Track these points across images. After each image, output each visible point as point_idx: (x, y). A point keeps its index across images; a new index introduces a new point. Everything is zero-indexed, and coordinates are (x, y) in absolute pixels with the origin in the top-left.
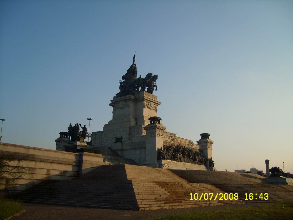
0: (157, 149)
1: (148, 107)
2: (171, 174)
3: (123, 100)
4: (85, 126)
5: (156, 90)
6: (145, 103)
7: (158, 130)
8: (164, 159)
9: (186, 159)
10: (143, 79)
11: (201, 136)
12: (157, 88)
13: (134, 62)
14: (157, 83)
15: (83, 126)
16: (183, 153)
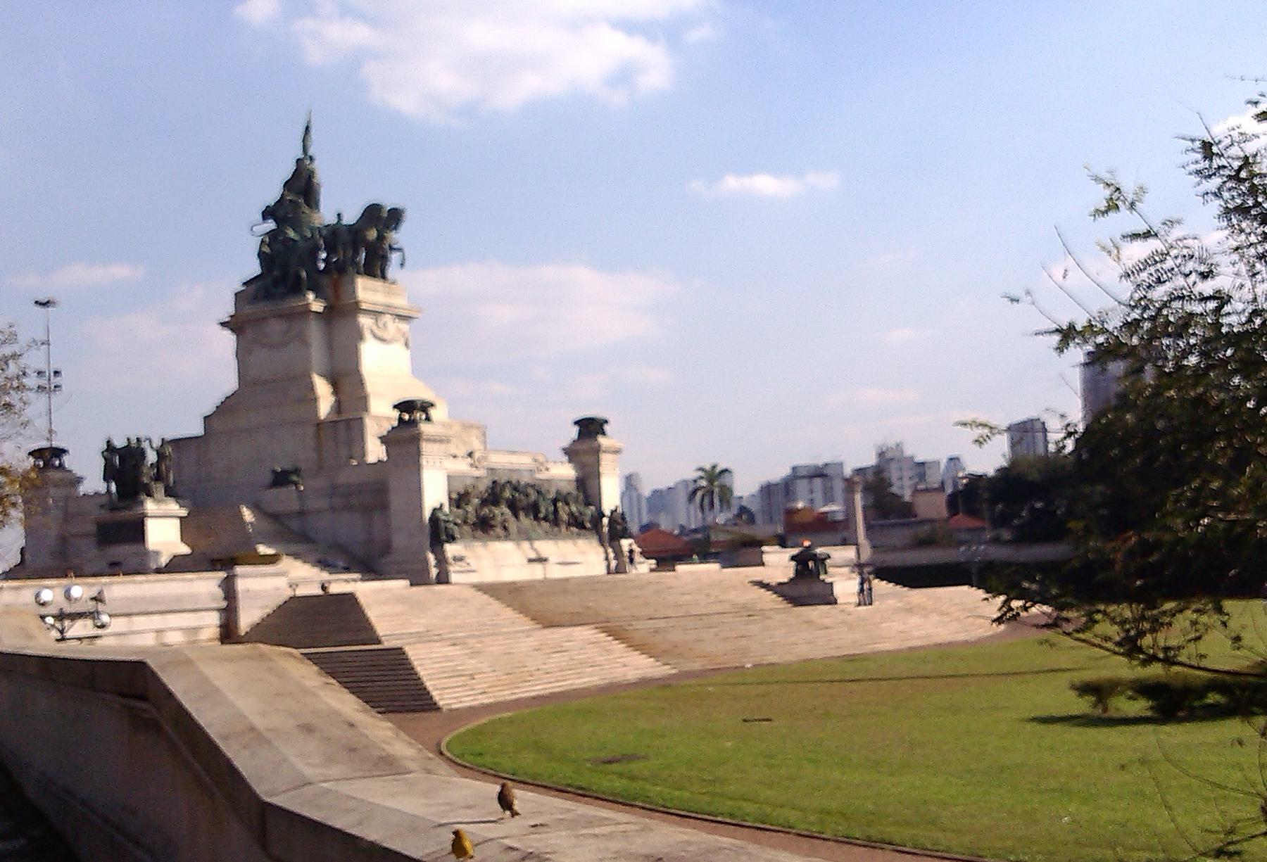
0: (427, 514)
1: (375, 336)
2: (484, 598)
3: (281, 316)
6: (365, 321)
7: (426, 447)
8: (452, 539)
9: (526, 521)
16: (514, 507)
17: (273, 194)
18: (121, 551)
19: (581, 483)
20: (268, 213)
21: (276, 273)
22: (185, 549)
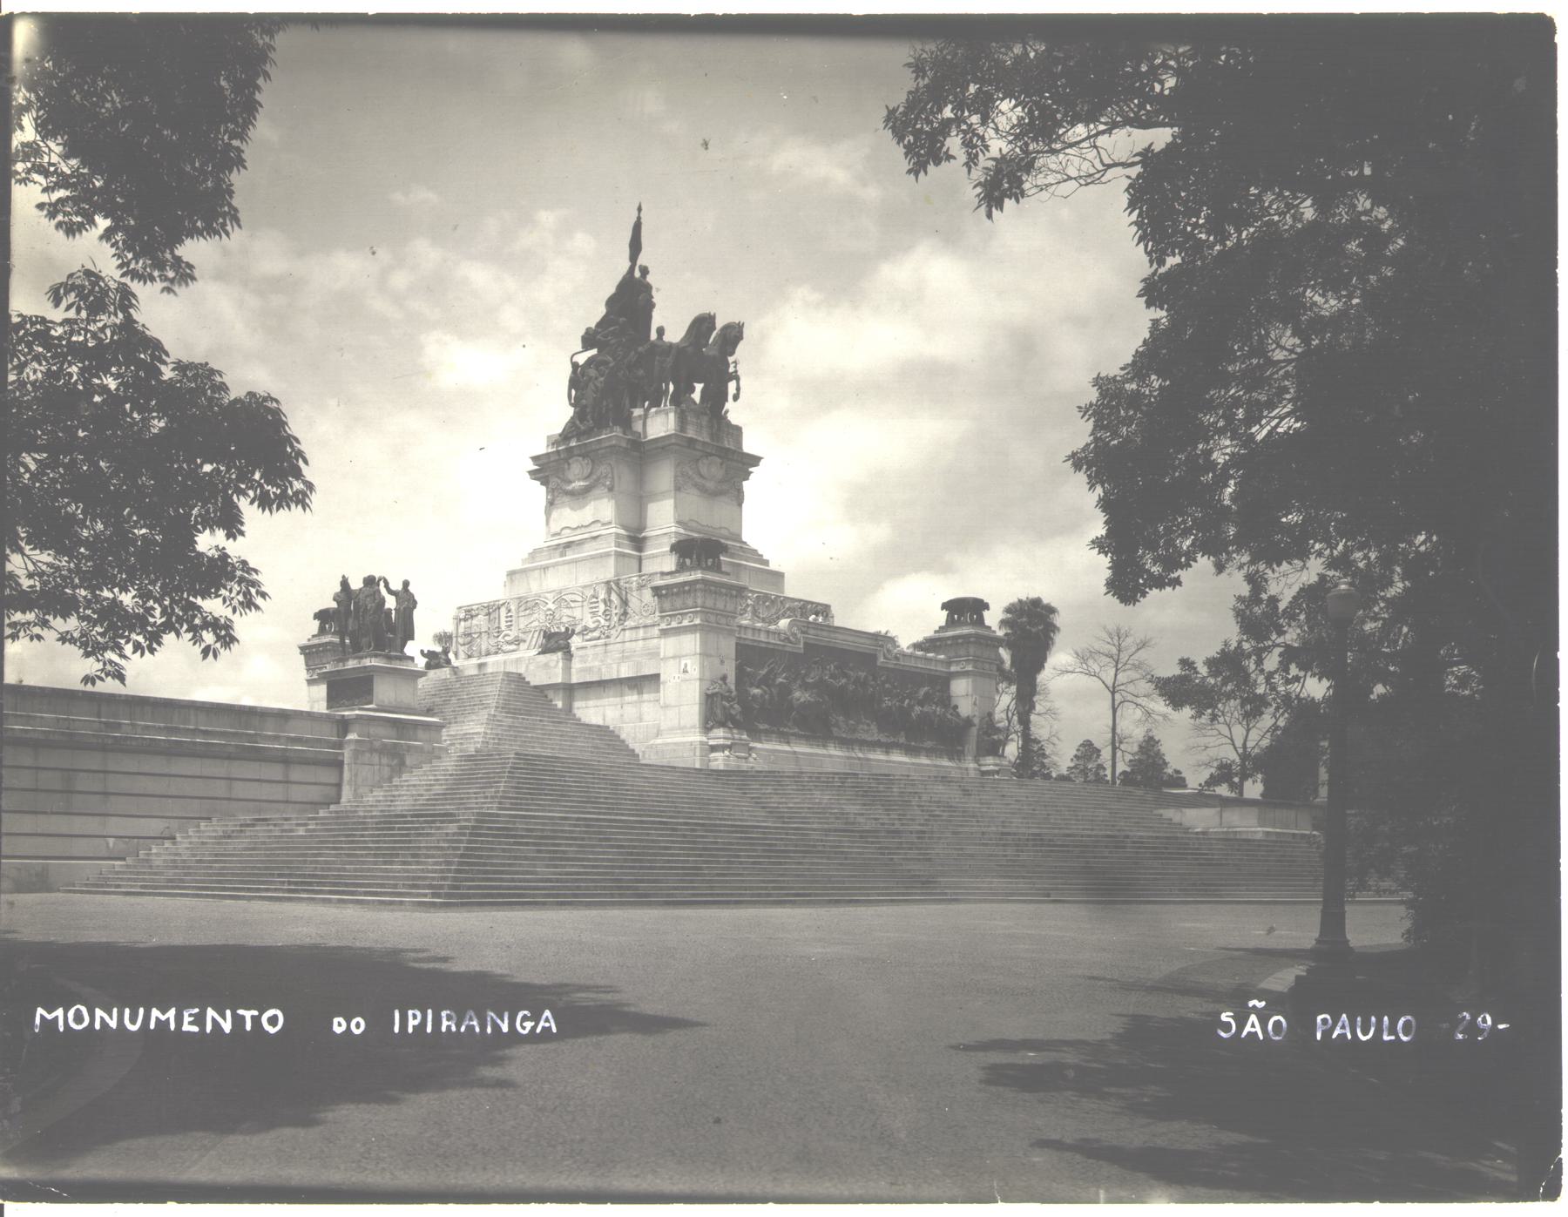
4: (406, 584)
5: (736, 398)
10: (671, 345)
11: (945, 613)
12: (738, 389)
13: (634, 257)
14: (742, 358)
15: (396, 585)
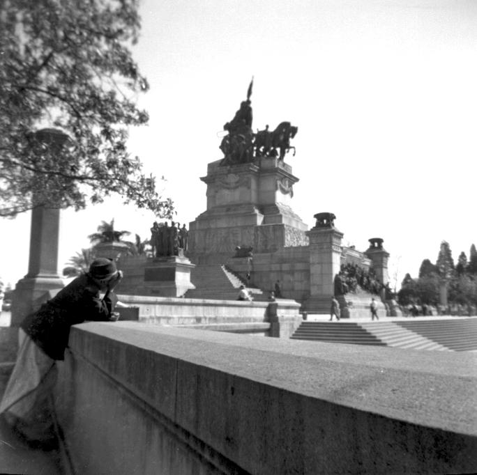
0: (334, 276)
5: (294, 155)
8: (346, 292)
17: (230, 117)
18: (163, 286)
19: (371, 269)
20: (227, 127)
21: (234, 152)
22: (192, 286)
